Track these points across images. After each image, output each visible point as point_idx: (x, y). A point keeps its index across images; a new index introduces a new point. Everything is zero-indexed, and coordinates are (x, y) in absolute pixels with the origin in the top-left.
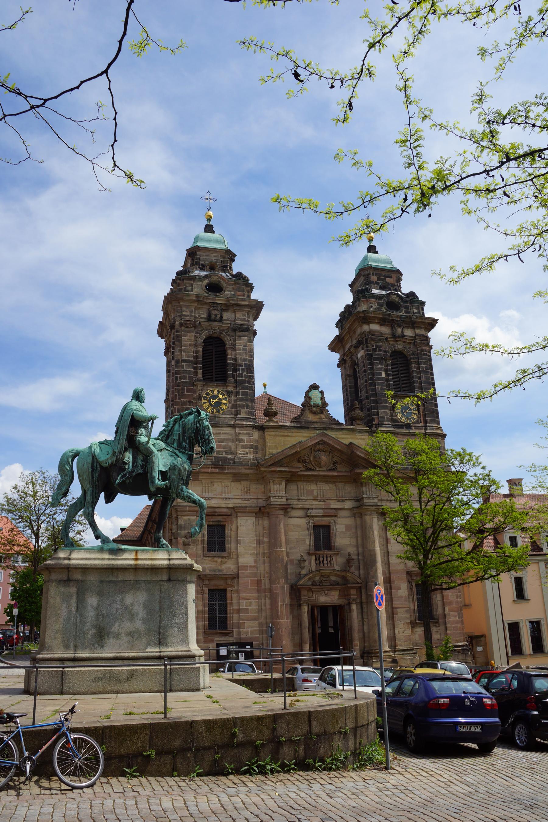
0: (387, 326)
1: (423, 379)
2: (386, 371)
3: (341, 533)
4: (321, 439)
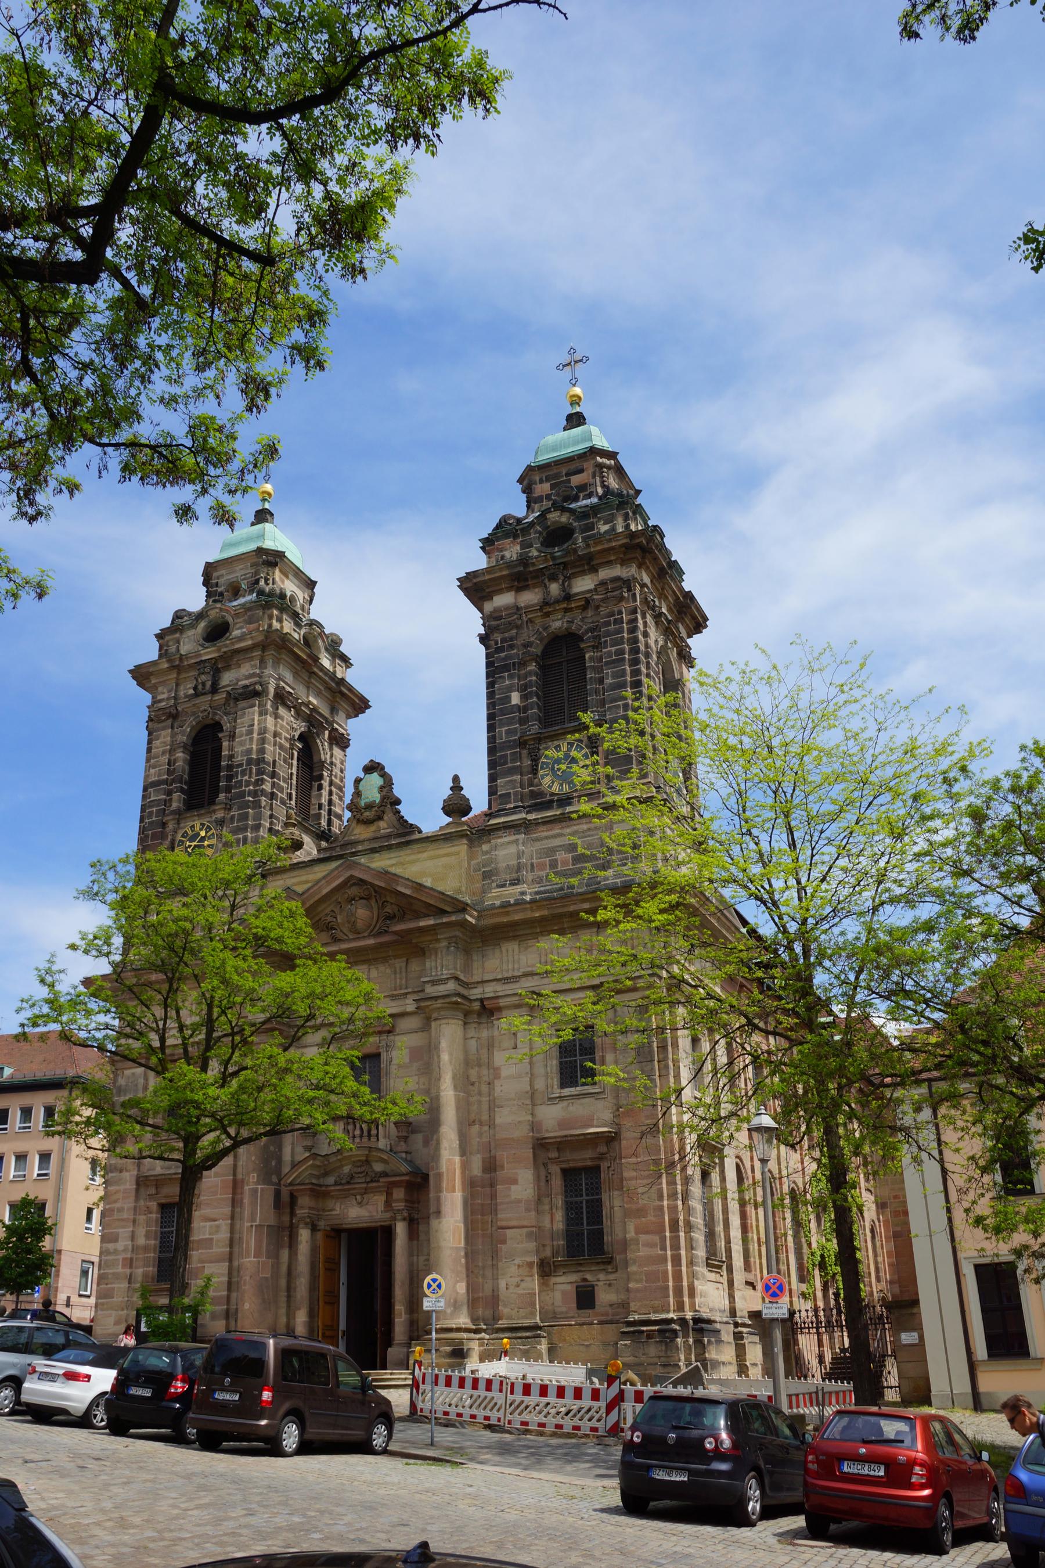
0: (534, 586)
1: (609, 681)
2: (523, 689)
3: (400, 1066)
4: (348, 874)
